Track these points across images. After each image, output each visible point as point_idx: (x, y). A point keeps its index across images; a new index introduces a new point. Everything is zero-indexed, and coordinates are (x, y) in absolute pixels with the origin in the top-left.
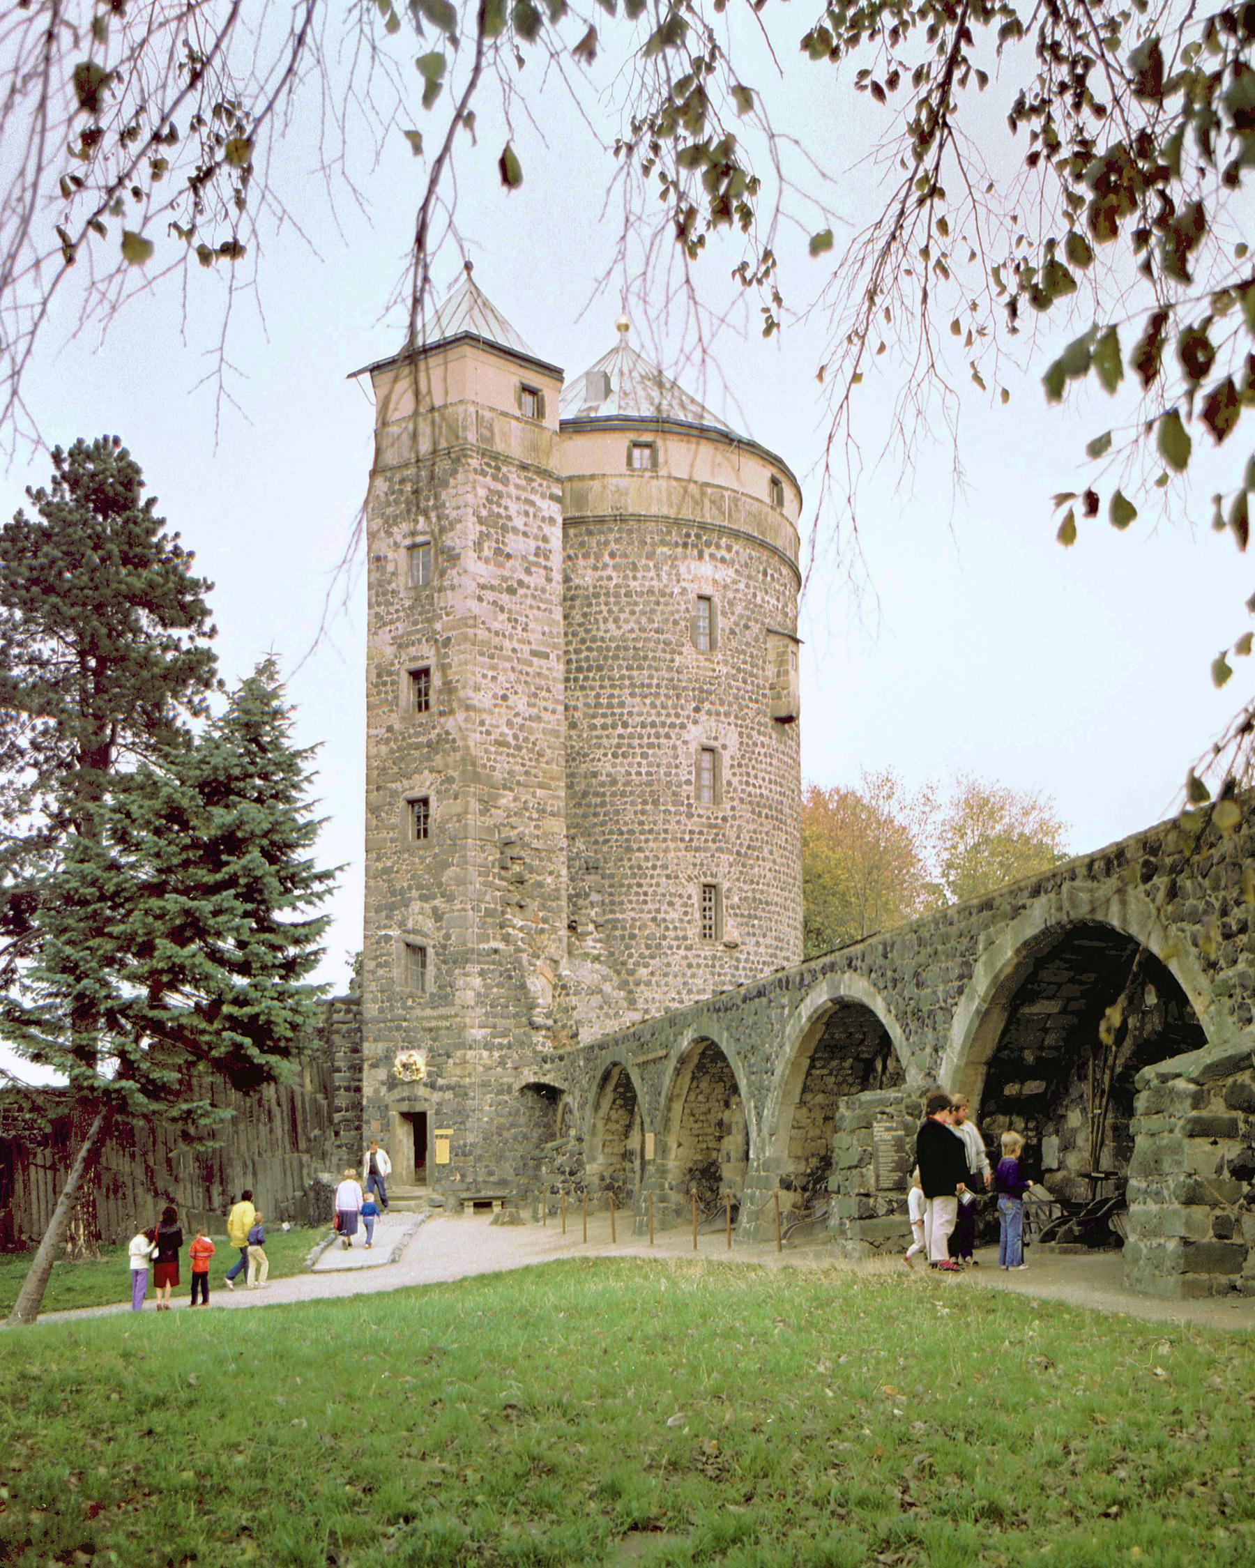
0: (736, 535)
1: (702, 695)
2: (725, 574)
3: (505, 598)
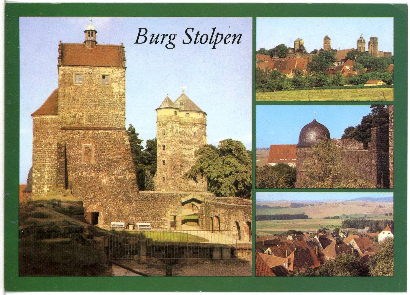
0: (199, 124)
1: (195, 144)
2: (198, 129)
3: (173, 137)
